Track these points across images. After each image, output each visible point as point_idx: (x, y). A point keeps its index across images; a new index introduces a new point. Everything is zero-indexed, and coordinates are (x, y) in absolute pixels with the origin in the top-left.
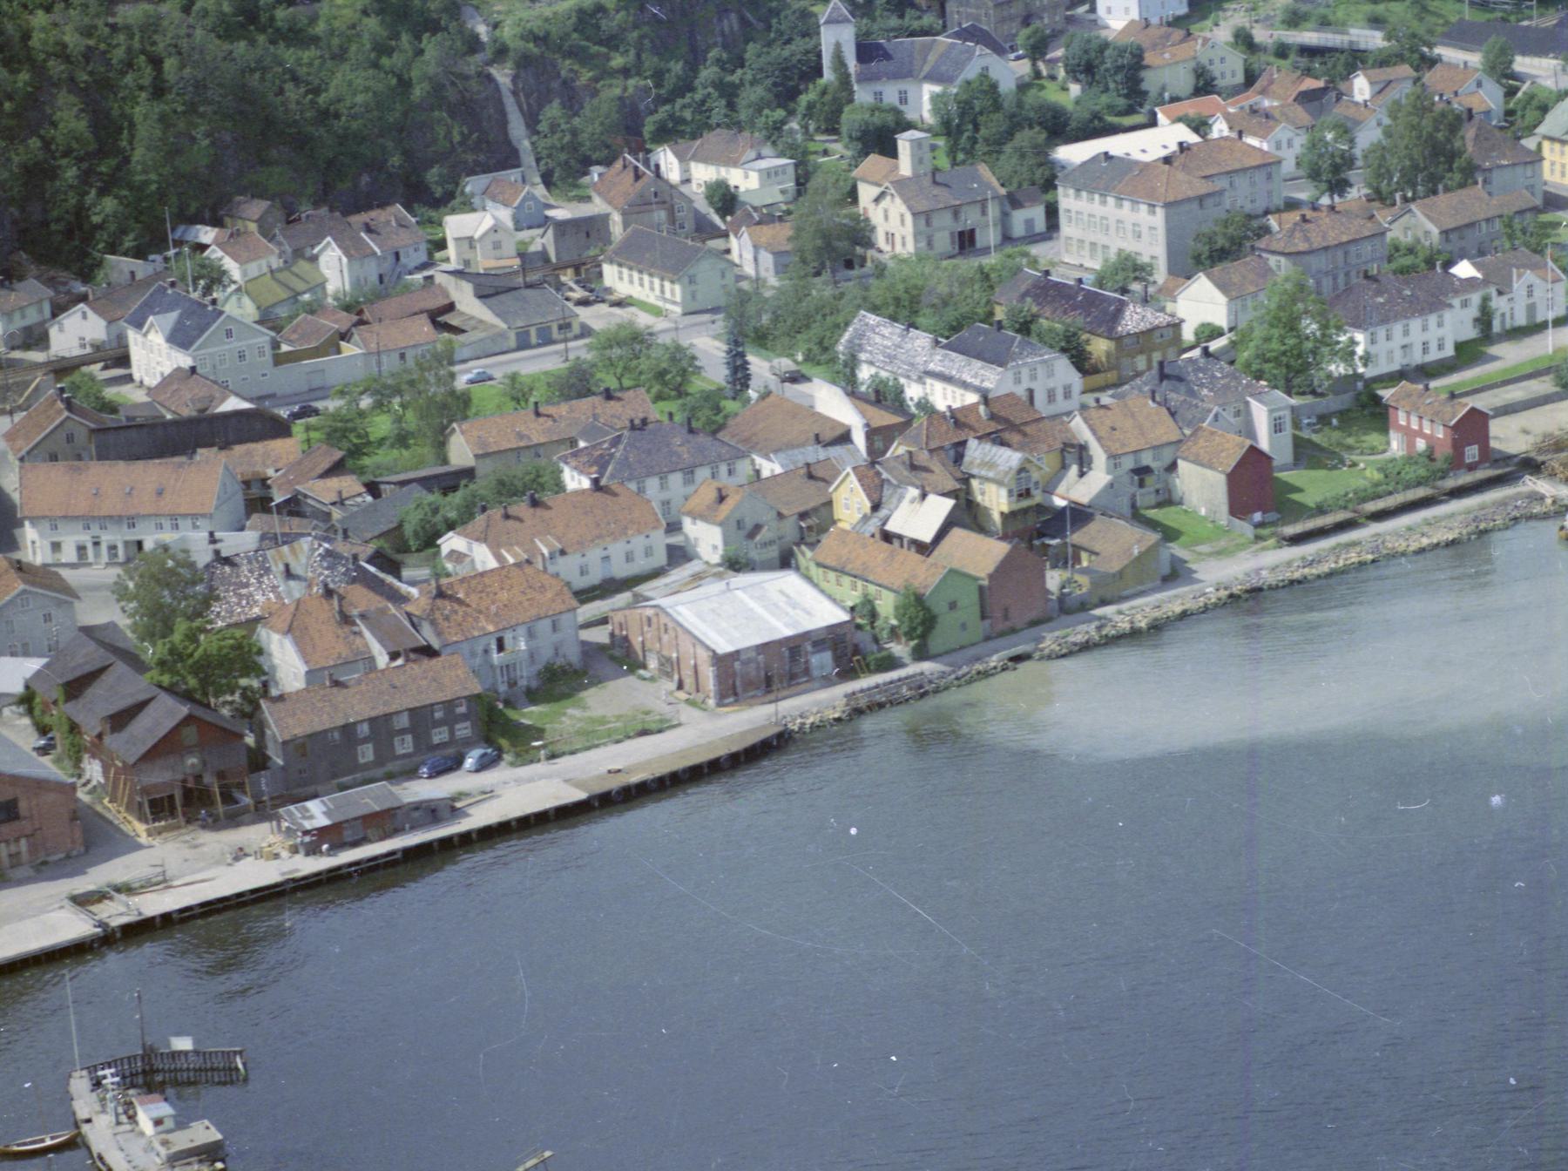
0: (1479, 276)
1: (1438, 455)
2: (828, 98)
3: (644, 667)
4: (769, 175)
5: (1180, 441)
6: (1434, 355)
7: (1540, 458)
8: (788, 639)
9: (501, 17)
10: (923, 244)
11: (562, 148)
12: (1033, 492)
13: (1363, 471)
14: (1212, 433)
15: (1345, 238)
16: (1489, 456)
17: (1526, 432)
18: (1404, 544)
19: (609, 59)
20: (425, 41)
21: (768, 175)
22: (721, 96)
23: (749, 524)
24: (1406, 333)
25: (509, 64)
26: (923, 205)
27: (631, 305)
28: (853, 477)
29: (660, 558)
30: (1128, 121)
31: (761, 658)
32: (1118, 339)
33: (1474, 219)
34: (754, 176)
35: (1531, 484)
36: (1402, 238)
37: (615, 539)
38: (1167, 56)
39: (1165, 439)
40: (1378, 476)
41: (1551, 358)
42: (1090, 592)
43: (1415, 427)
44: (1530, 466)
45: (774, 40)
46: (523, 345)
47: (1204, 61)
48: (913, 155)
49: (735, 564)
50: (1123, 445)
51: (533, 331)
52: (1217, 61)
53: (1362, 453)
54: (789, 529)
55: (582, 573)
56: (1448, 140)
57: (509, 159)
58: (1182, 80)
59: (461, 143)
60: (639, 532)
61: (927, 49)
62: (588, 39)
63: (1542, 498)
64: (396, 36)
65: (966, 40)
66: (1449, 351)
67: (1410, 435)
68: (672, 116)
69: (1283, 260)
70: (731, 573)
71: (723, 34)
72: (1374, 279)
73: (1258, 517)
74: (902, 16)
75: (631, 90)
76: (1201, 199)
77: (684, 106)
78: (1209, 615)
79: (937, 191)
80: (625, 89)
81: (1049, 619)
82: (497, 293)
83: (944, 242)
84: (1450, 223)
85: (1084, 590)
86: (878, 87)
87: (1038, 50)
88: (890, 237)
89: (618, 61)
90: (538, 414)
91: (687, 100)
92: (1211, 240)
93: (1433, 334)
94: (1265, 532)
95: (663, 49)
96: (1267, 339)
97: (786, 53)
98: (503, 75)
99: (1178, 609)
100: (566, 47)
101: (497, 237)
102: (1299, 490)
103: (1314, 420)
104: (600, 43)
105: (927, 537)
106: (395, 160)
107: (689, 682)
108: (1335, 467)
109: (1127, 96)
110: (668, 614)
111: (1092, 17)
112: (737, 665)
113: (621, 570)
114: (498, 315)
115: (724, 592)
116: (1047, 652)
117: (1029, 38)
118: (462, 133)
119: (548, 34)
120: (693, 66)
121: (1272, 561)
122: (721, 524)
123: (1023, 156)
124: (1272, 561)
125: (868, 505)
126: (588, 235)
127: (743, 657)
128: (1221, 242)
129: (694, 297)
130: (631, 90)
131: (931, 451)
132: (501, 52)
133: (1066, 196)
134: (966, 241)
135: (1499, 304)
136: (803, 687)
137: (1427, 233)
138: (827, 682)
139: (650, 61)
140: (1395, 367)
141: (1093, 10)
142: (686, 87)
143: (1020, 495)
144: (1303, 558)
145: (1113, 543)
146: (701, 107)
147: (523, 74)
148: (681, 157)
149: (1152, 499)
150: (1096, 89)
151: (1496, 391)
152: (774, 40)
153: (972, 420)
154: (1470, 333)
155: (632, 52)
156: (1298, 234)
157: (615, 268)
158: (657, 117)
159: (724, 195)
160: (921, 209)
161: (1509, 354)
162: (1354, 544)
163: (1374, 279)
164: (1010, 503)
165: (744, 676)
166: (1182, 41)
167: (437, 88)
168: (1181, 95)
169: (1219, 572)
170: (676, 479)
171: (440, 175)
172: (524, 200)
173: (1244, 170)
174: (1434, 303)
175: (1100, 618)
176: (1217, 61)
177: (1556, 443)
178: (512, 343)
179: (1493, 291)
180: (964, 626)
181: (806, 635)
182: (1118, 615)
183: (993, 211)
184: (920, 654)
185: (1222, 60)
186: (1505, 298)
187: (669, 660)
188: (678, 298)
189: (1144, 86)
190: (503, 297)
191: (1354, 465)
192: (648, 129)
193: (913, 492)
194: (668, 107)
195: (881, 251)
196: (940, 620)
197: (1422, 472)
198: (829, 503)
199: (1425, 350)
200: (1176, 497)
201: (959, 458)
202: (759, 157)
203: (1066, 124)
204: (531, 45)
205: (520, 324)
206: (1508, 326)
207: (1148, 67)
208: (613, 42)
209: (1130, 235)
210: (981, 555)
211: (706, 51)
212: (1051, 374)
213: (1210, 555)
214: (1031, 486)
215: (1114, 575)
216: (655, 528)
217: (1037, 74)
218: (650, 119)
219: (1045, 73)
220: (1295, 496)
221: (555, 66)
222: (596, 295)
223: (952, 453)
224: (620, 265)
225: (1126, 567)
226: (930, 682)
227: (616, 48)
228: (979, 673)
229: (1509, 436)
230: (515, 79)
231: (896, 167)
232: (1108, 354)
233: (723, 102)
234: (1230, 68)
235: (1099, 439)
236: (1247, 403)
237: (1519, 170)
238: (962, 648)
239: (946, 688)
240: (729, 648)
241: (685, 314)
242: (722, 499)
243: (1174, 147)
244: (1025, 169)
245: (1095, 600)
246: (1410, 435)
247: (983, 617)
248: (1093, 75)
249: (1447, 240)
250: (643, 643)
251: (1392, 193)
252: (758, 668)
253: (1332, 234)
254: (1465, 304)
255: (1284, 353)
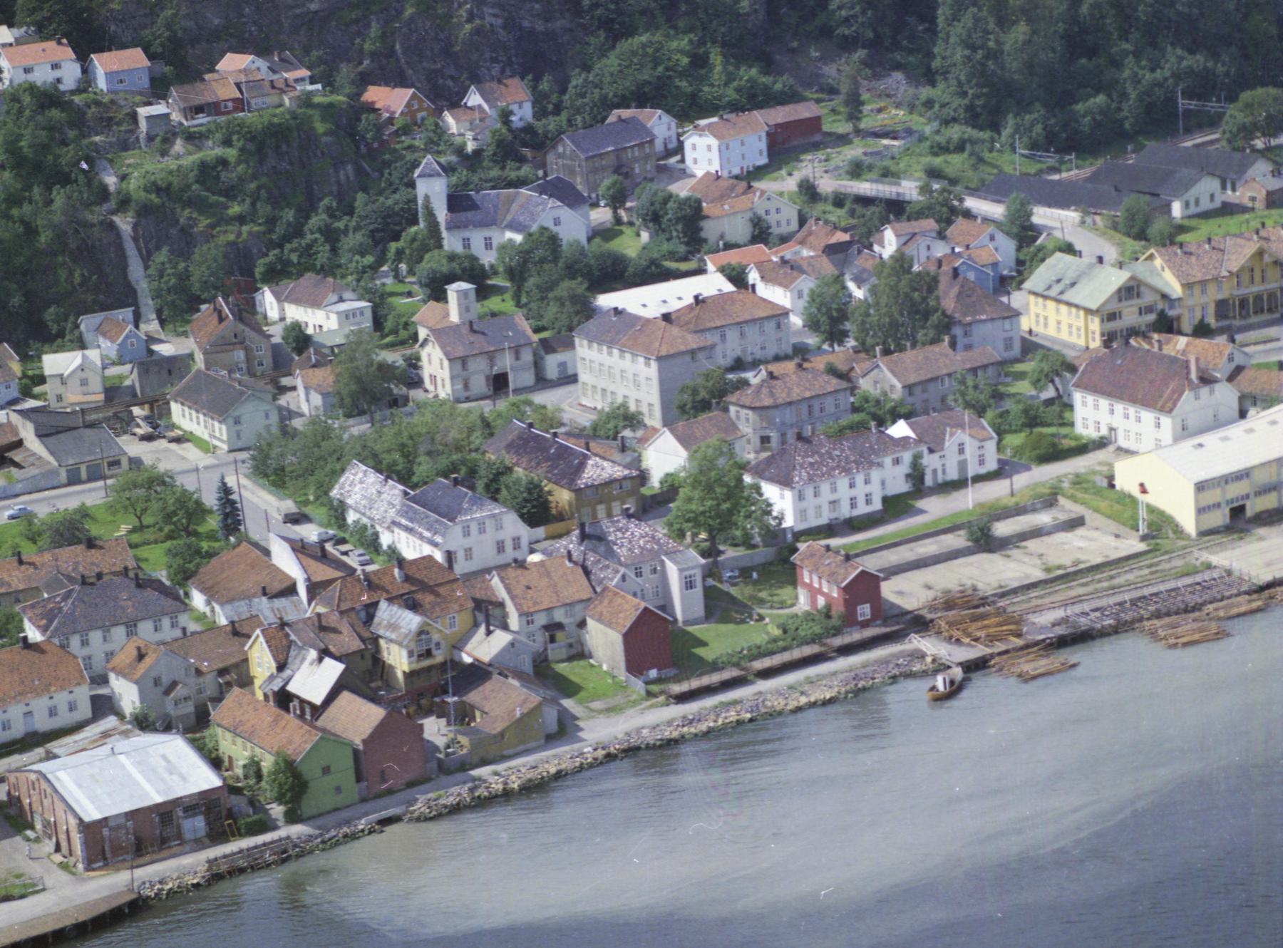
0: (913, 435)
1: (833, 613)
2: (416, 245)
3: (32, 828)
4: (347, 317)
5: (589, 600)
6: (862, 509)
7: (929, 616)
8: (157, 806)
9: (130, 170)
10: (460, 386)
11: (169, 290)
12: (434, 652)
13: (764, 628)
14: (616, 594)
15: (808, 394)
16: (884, 613)
17: (929, 587)
18: (783, 703)
19: (227, 208)
20: (55, 193)
21: (346, 316)
22: (326, 241)
23: (166, 681)
24: (834, 490)
25: (131, 214)
26: (460, 351)
27: (188, 441)
28: (261, 639)
29: (85, 711)
30: (684, 266)
31: (130, 824)
32: (578, 491)
33: (937, 374)
34: (334, 317)
35: (917, 642)
36: (872, 391)
37: (38, 695)
38: (726, 207)
39: (577, 597)
40: (777, 632)
41: (970, 513)
42: (470, 753)
43: (816, 585)
44: (919, 623)
45: (384, 189)
46: (74, 480)
47: (761, 212)
48: (459, 305)
49: (143, 723)
50: (536, 603)
51: (83, 469)
52: (773, 211)
53: (772, 607)
54: (210, 684)
55: (71, 710)
56: (924, 299)
57: (125, 296)
58: (739, 228)
59: (81, 285)
60: (62, 688)
61: (511, 200)
62: (208, 190)
63: (922, 656)
64: (28, 188)
65: (541, 194)
66: (877, 505)
67: (814, 592)
68: (280, 259)
69: (750, 413)
70: (138, 732)
71: (338, 182)
72: (806, 441)
73: (653, 673)
74: (503, 168)
75: (245, 235)
76: (693, 353)
77: (292, 250)
78: (613, 766)
79: (472, 338)
80: (239, 234)
81: (429, 780)
82: (58, 433)
83: (479, 384)
84: (913, 379)
85: (465, 751)
86: (467, 234)
87: (617, 200)
88: (433, 378)
89: (235, 209)
90: (21, 562)
91: (294, 245)
92: (695, 392)
93: (860, 490)
94: (655, 688)
95: (277, 201)
96: (690, 500)
97: (390, 202)
98: (124, 223)
99: (553, 770)
100: (186, 196)
101: (83, 375)
102: (703, 644)
103: (736, 573)
104: (220, 193)
105: (318, 700)
106: (16, 301)
107: (64, 844)
108: (743, 622)
109: (687, 244)
110: (48, 781)
111: (681, 166)
112: (106, 832)
113: (43, 723)
114: (52, 453)
115: (108, 756)
116: (416, 814)
117: (609, 188)
118: (83, 275)
119: (170, 184)
120: (306, 212)
121: (653, 719)
122: (136, 682)
123: (563, 305)
124: (653, 719)
125: (274, 665)
126: (170, 372)
127: (112, 824)
128: (703, 394)
129: (239, 436)
130: (245, 235)
131: (342, 613)
132: (124, 203)
133: (581, 346)
134: (499, 383)
135: (930, 462)
136: (175, 850)
137: (892, 387)
138: (199, 845)
139: (264, 209)
140: (824, 520)
141: (683, 161)
142: (296, 231)
143: (420, 656)
144: (684, 717)
145: (502, 702)
146: (308, 251)
147: (143, 221)
148: (278, 296)
149: (563, 653)
150: (663, 237)
151: (912, 545)
152: (384, 189)
153: (385, 581)
154: (899, 485)
155: (248, 201)
156: (765, 391)
157: (179, 406)
158: (267, 260)
159: (297, 337)
160: (457, 355)
161: (934, 508)
162: (735, 703)
163: (806, 441)
164: (410, 663)
165: (109, 842)
166: (743, 194)
167: (60, 236)
168: (741, 241)
169: (601, 730)
170: (119, 632)
171: (57, 314)
172: (127, 337)
173: (753, 321)
174: (866, 460)
175: (474, 779)
176: (773, 211)
177: (946, 602)
178: (63, 476)
179: (925, 449)
180: (338, 790)
181: (176, 802)
182: (490, 776)
183: (527, 356)
184: (292, 818)
185: (778, 211)
186: (936, 456)
187: (49, 823)
188: (225, 437)
189: (703, 235)
190: (61, 436)
191: (761, 618)
192: (258, 271)
193: (313, 654)
194: (276, 251)
195: (426, 391)
196: (311, 784)
197: (817, 629)
198: (246, 660)
199: (853, 505)
200: (586, 653)
201: (370, 618)
202: (341, 300)
203: (625, 270)
204: (153, 196)
205: (71, 462)
206: (940, 480)
207: (707, 217)
208: (230, 193)
209: (631, 384)
210: (359, 718)
211: (321, 200)
212: (499, 527)
213: (601, 712)
214: (433, 646)
215: (495, 736)
216: (79, 684)
217: (618, 221)
218: (262, 261)
219: (625, 219)
220: (700, 651)
221: (173, 213)
222: (159, 427)
223: (363, 614)
224: (183, 404)
225: (507, 728)
226: (296, 846)
227: (234, 198)
228: (346, 836)
229: (905, 592)
230: (135, 227)
231: (447, 315)
232: (570, 504)
233: (328, 247)
234: (784, 217)
235: (513, 598)
236: (662, 562)
237: (998, 324)
238: (336, 810)
239: (311, 852)
240: (97, 816)
241: (231, 451)
242: (141, 656)
243: (689, 300)
244: (564, 316)
245: (475, 760)
246: (814, 592)
247: (359, 779)
248: (660, 224)
249: (910, 394)
250: (30, 804)
251: (873, 347)
252: (128, 833)
253: (796, 390)
254: (897, 461)
255: (703, 513)
